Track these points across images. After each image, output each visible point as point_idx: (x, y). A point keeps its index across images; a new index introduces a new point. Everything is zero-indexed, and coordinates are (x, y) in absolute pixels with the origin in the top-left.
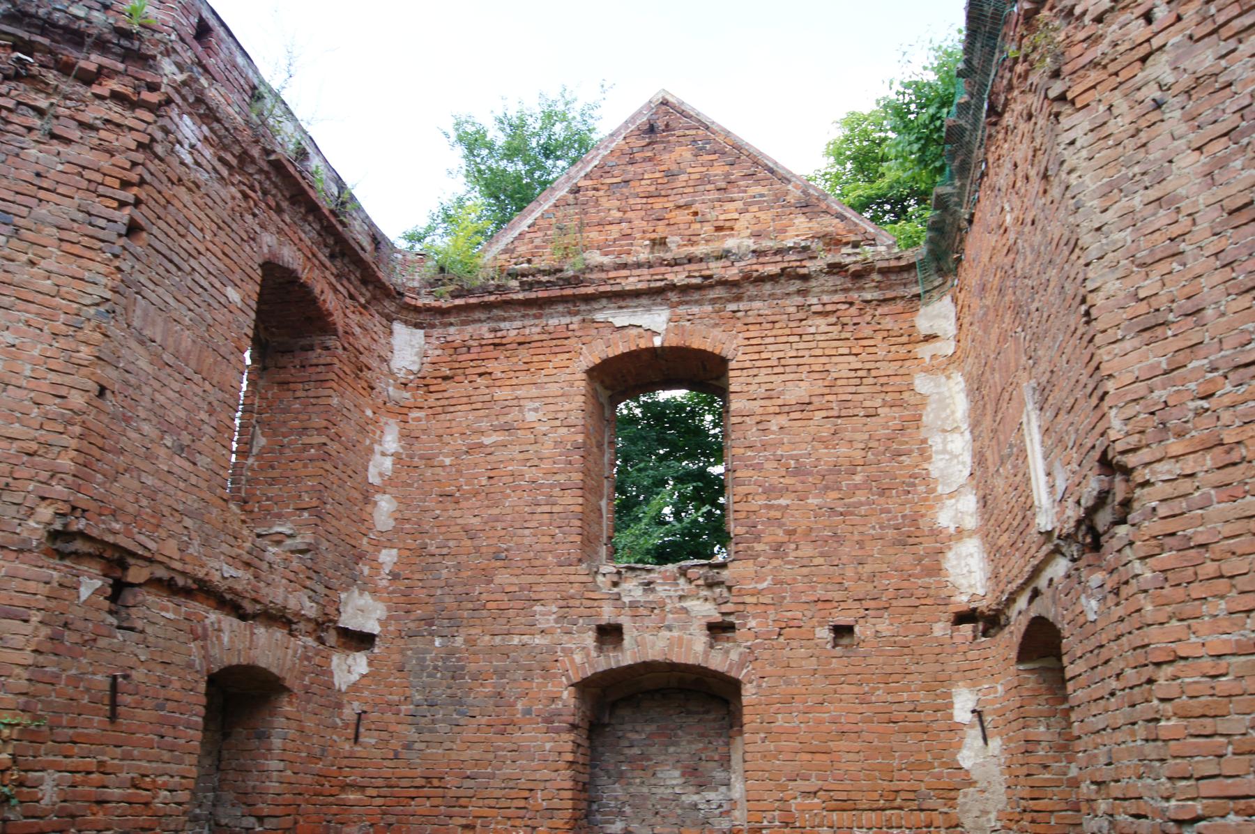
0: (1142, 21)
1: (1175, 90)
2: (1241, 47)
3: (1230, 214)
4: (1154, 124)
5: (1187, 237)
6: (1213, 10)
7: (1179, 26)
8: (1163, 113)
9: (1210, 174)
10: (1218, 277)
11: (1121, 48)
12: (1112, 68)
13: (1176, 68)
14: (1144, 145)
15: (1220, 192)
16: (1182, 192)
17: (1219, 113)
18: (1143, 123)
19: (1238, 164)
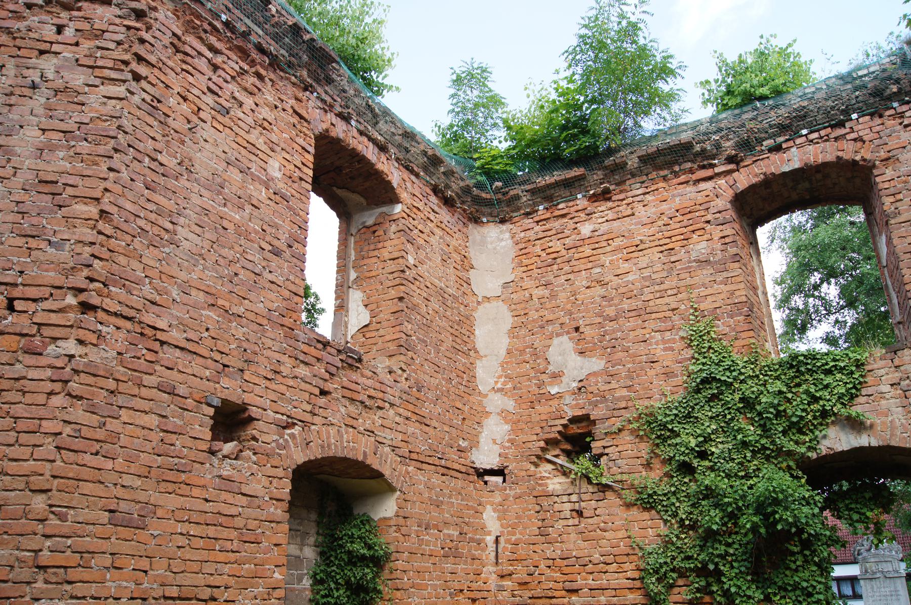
0: (54, 28)
1: (49, 84)
2: (102, 87)
3: (39, 182)
4: (25, 96)
5: (5, 181)
6: (98, 55)
7: (74, 48)
8: (34, 93)
9: (42, 150)
10: (11, 218)
11: (32, 35)
12: (19, 42)
13: (57, 72)
14: (11, 105)
15: (41, 165)
16: (18, 150)
17: (67, 117)
18: (18, 91)
19: (61, 154)
